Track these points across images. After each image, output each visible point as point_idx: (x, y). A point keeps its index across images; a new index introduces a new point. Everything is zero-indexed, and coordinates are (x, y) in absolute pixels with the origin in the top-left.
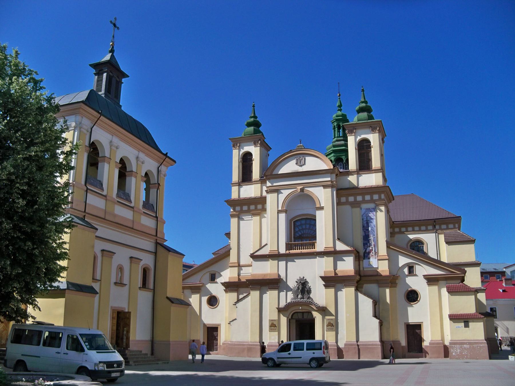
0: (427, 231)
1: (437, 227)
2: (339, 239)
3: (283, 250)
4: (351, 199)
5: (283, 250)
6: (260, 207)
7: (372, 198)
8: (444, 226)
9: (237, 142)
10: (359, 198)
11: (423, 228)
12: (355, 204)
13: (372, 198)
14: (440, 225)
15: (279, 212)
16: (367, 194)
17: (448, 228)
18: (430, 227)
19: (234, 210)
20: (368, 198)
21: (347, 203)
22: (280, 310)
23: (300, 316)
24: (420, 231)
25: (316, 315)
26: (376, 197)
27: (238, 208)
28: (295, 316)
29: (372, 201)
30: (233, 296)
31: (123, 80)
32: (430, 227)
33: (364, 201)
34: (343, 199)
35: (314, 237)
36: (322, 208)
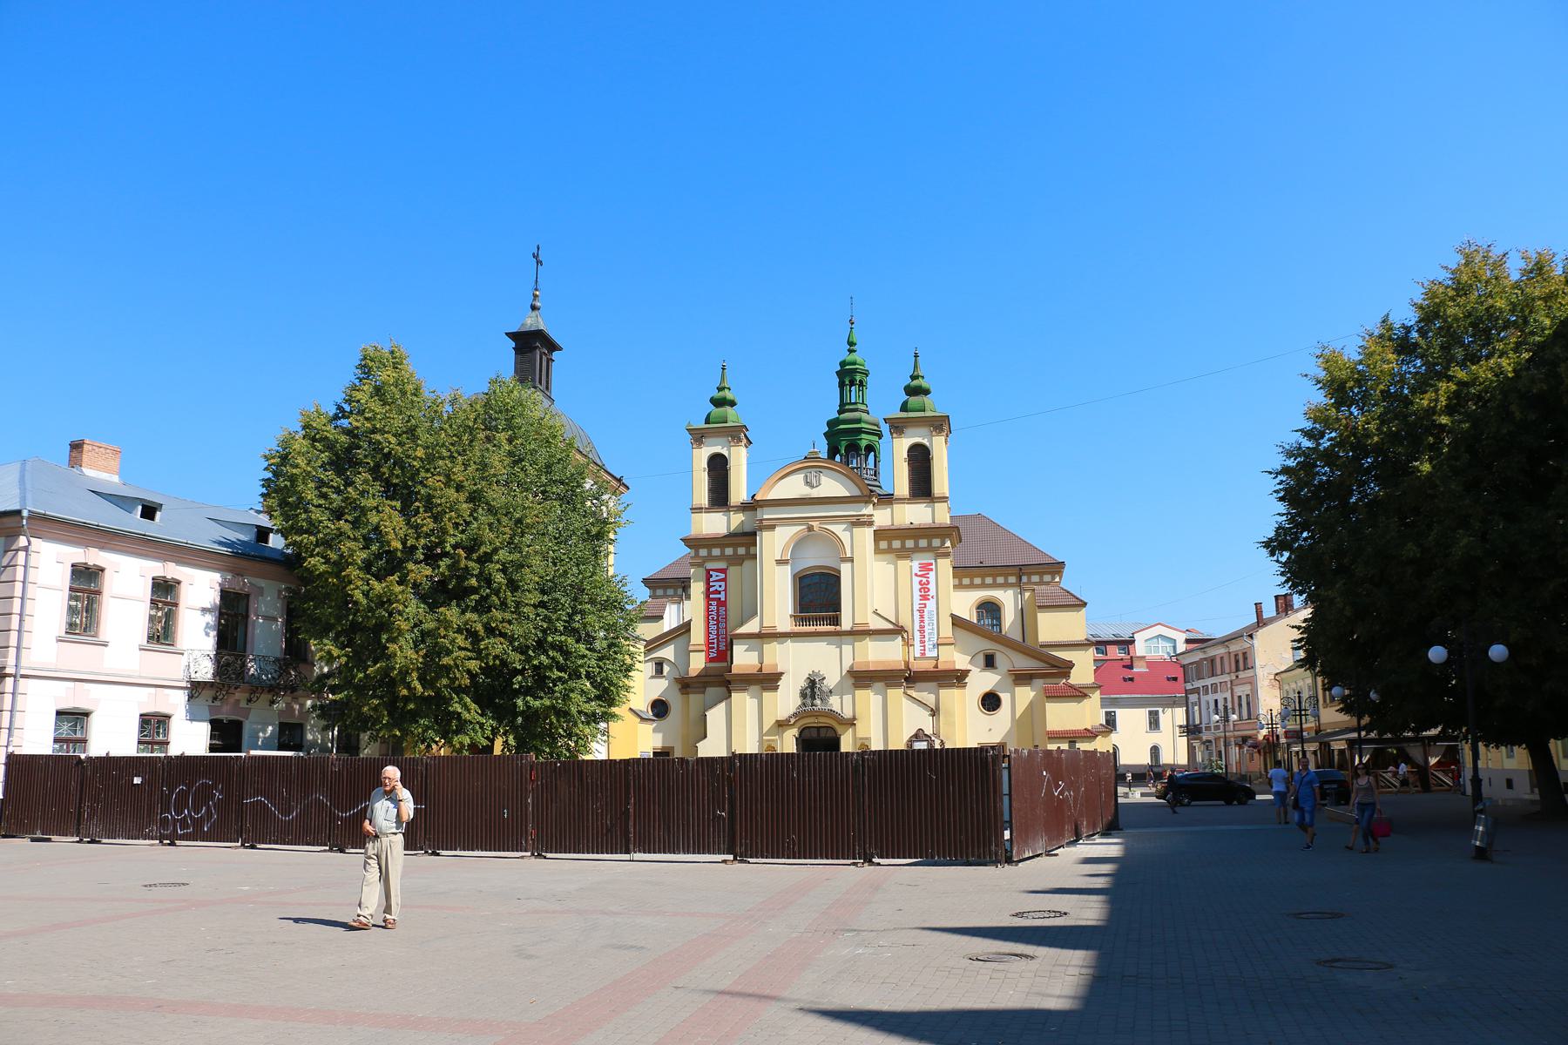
0: (1006, 585)
1: (1024, 579)
2: (875, 612)
3: (785, 623)
4: (897, 544)
5: (785, 623)
6: (741, 551)
7: (930, 544)
8: (1035, 578)
9: (699, 437)
10: (910, 544)
11: (1000, 580)
12: (903, 553)
13: (930, 544)
14: (1030, 575)
15: (780, 562)
16: (923, 537)
17: (1041, 583)
18: (1012, 579)
19: (697, 555)
20: (923, 543)
21: (890, 550)
22: (781, 725)
23: (814, 734)
24: (995, 586)
25: (839, 729)
26: (936, 542)
27: (703, 552)
28: (806, 734)
29: (929, 549)
30: (695, 699)
31: (555, 355)
32: (1012, 579)
33: (917, 549)
34: (883, 545)
35: (836, 606)
36: (851, 560)
